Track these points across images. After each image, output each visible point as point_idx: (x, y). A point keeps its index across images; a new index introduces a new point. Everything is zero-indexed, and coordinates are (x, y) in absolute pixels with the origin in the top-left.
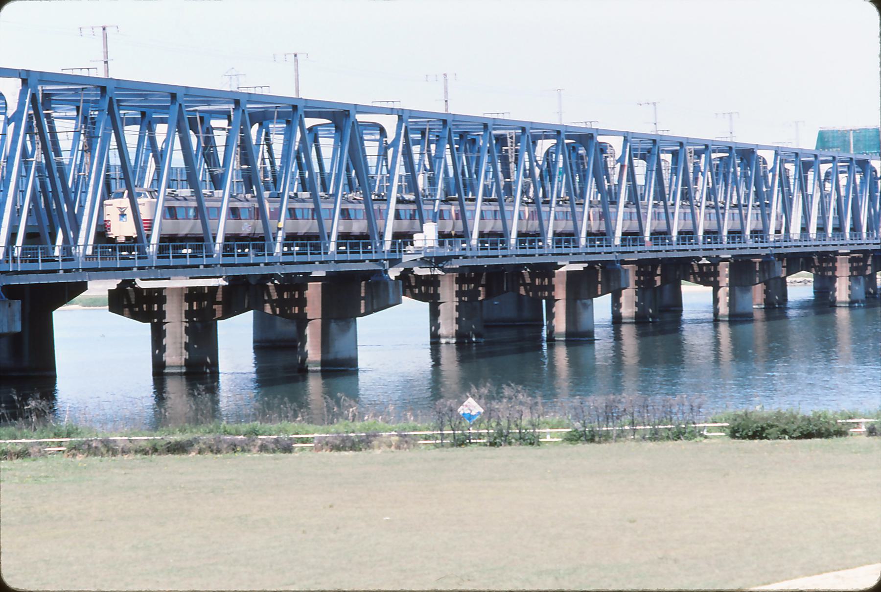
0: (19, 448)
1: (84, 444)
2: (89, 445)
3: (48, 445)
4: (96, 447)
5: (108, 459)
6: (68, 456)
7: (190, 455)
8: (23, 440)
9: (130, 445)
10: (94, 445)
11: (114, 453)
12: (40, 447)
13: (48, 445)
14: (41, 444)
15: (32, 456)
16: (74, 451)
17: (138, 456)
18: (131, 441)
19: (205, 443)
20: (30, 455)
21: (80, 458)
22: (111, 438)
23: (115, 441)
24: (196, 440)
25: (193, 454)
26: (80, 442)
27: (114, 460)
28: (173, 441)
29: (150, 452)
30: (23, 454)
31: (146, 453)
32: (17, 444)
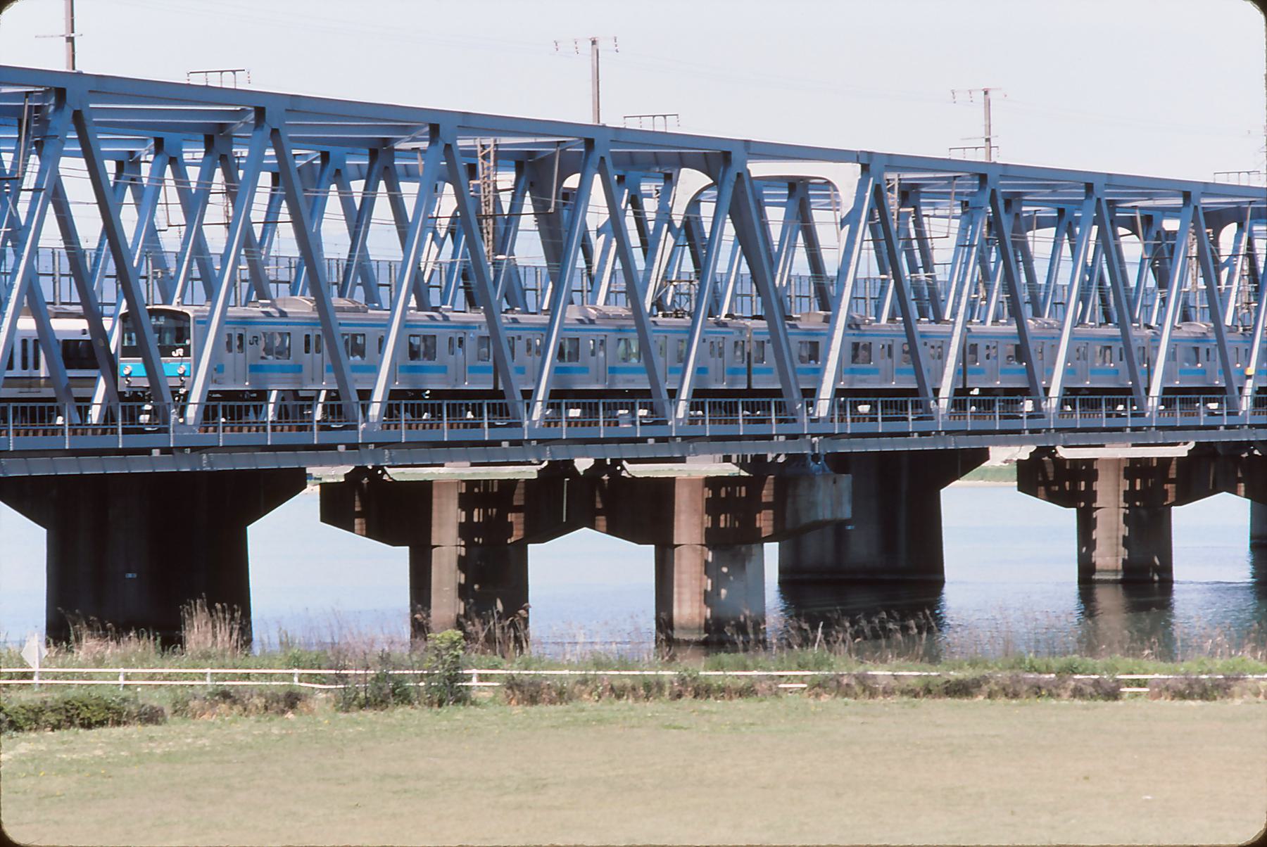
0: (741, 683)
1: (831, 679)
2: (838, 682)
3: (789, 680)
4: (848, 685)
5: (865, 700)
6: (810, 695)
7: (976, 700)
8: (755, 673)
9: (893, 683)
10: (845, 681)
11: (873, 694)
12: (769, 682)
13: (789, 680)
14: (772, 677)
15: (759, 695)
16: (817, 689)
17: (905, 698)
18: (896, 677)
19: (997, 683)
20: (757, 694)
21: (825, 698)
22: (869, 673)
23: (874, 676)
24: (986, 679)
25: (981, 698)
26: (826, 677)
27: (866, 704)
28: (952, 679)
29: (921, 693)
30: (747, 692)
31: (916, 695)
32: (738, 677)
